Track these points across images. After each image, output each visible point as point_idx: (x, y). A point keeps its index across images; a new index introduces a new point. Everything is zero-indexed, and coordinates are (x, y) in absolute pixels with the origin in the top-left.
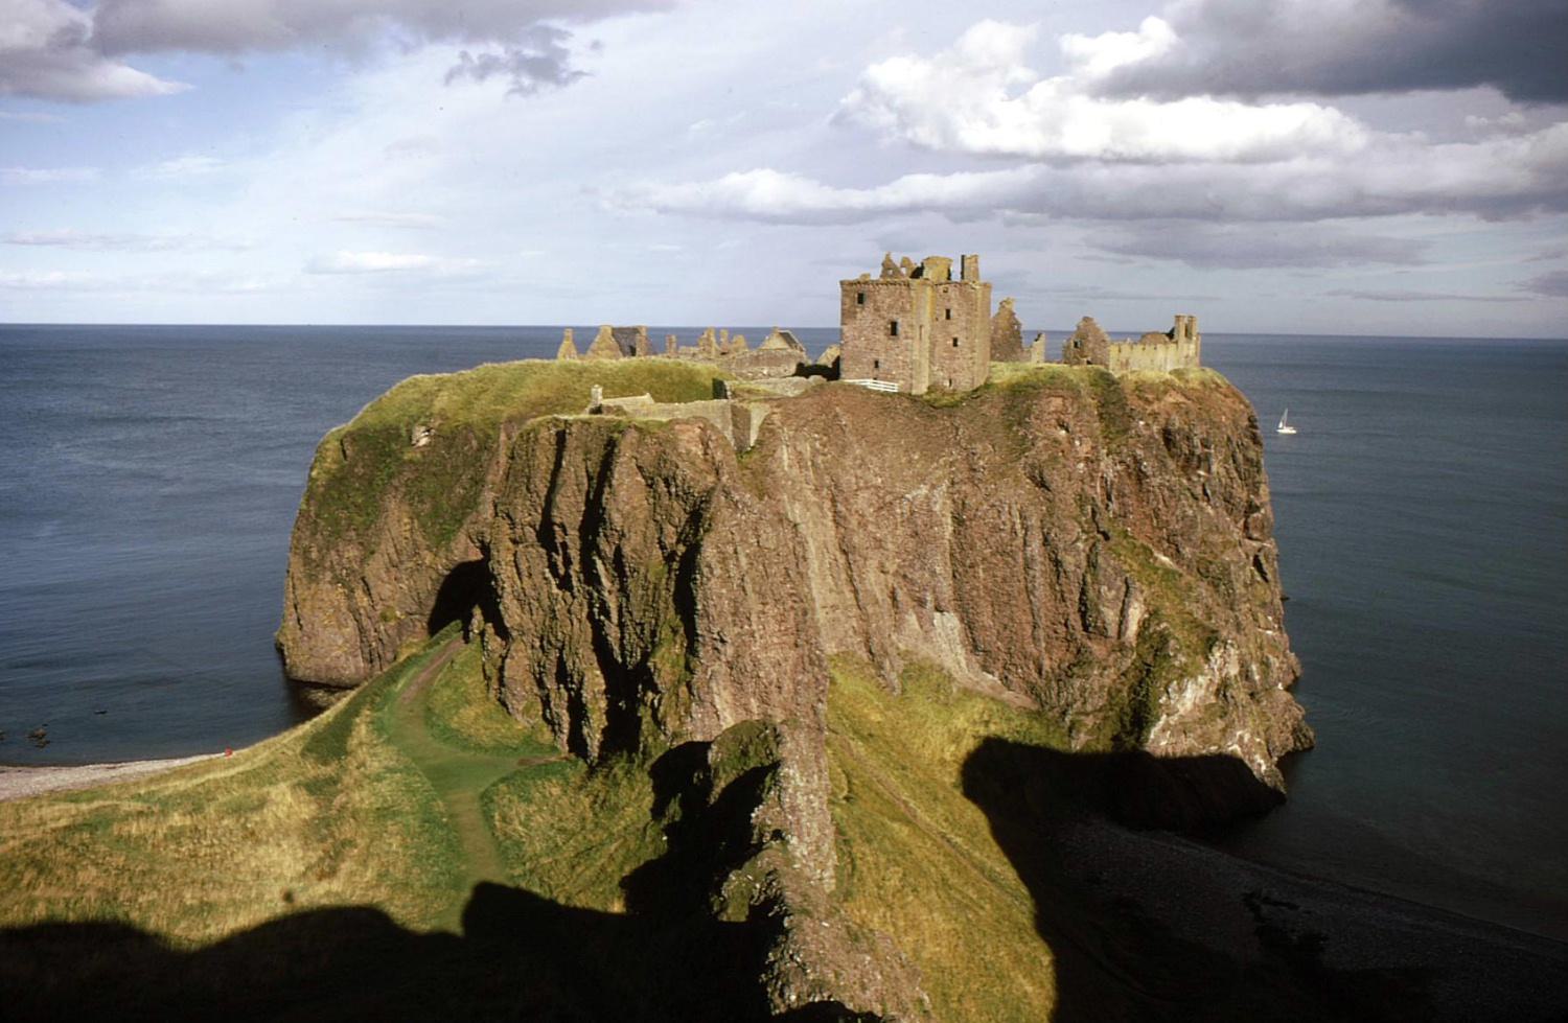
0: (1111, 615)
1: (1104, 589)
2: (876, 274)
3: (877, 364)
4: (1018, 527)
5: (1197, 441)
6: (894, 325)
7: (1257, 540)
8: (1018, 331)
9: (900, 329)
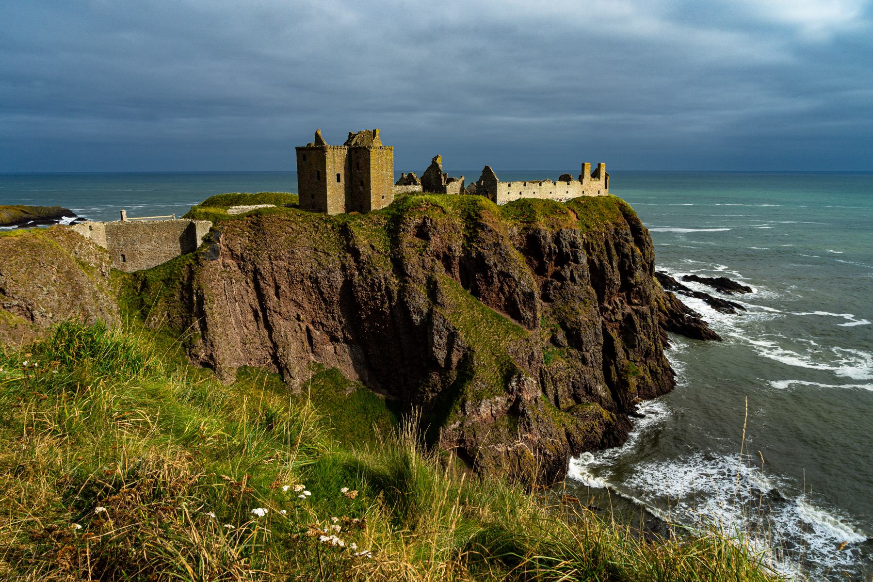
0: (440, 355)
1: (436, 338)
2: (313, 145)
3: (313, 196)
6: (318, 173)
7: (636, 304)
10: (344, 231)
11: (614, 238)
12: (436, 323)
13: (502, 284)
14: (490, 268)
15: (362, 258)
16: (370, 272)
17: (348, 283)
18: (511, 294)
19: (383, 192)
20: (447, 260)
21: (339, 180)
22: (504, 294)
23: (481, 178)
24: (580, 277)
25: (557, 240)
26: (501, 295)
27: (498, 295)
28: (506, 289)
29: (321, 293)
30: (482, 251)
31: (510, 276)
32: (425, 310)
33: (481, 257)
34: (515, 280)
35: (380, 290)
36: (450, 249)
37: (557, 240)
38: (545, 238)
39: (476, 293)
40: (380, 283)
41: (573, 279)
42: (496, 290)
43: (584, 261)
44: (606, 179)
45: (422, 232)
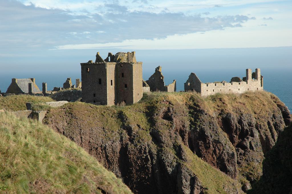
1: (184, 181)
2: (94, 61)
3: (94, 95)
4: (149, 157)
5: (245, 123)
6: (100, 80)
8: (162, 80)
9: (102, 81)
10: (121, 116)
11: (273, 120)
12: (183, 171)
13: (215, 148)
14: (208, 137)
15: (133, 132)
16: (139, 142)
17: (124, 150)
18: (221, 155)
19: (139, 90)
20: (182, 133)
21: (112, 85)
22: (216, 155)
23: (188, 81)
24: (255, 146)
25: (240, 122)
26: (214, 156)
27: (213, 155)
28: (218, 151)
29: (107, 157)
30: (203, 127)
31: (220, 143)
32: (175, 164)
33: (202, 131)
34: (223, 145)
35: (145, 153)
36: (184, 126)
37: (240, 122)
38: (233, 120)
39: (200, 155)
40: (145, 149)
41: (251, 148)
42: (212, 152)
43: (257, 134)
44: (261, 79)
45: (167, 117)
